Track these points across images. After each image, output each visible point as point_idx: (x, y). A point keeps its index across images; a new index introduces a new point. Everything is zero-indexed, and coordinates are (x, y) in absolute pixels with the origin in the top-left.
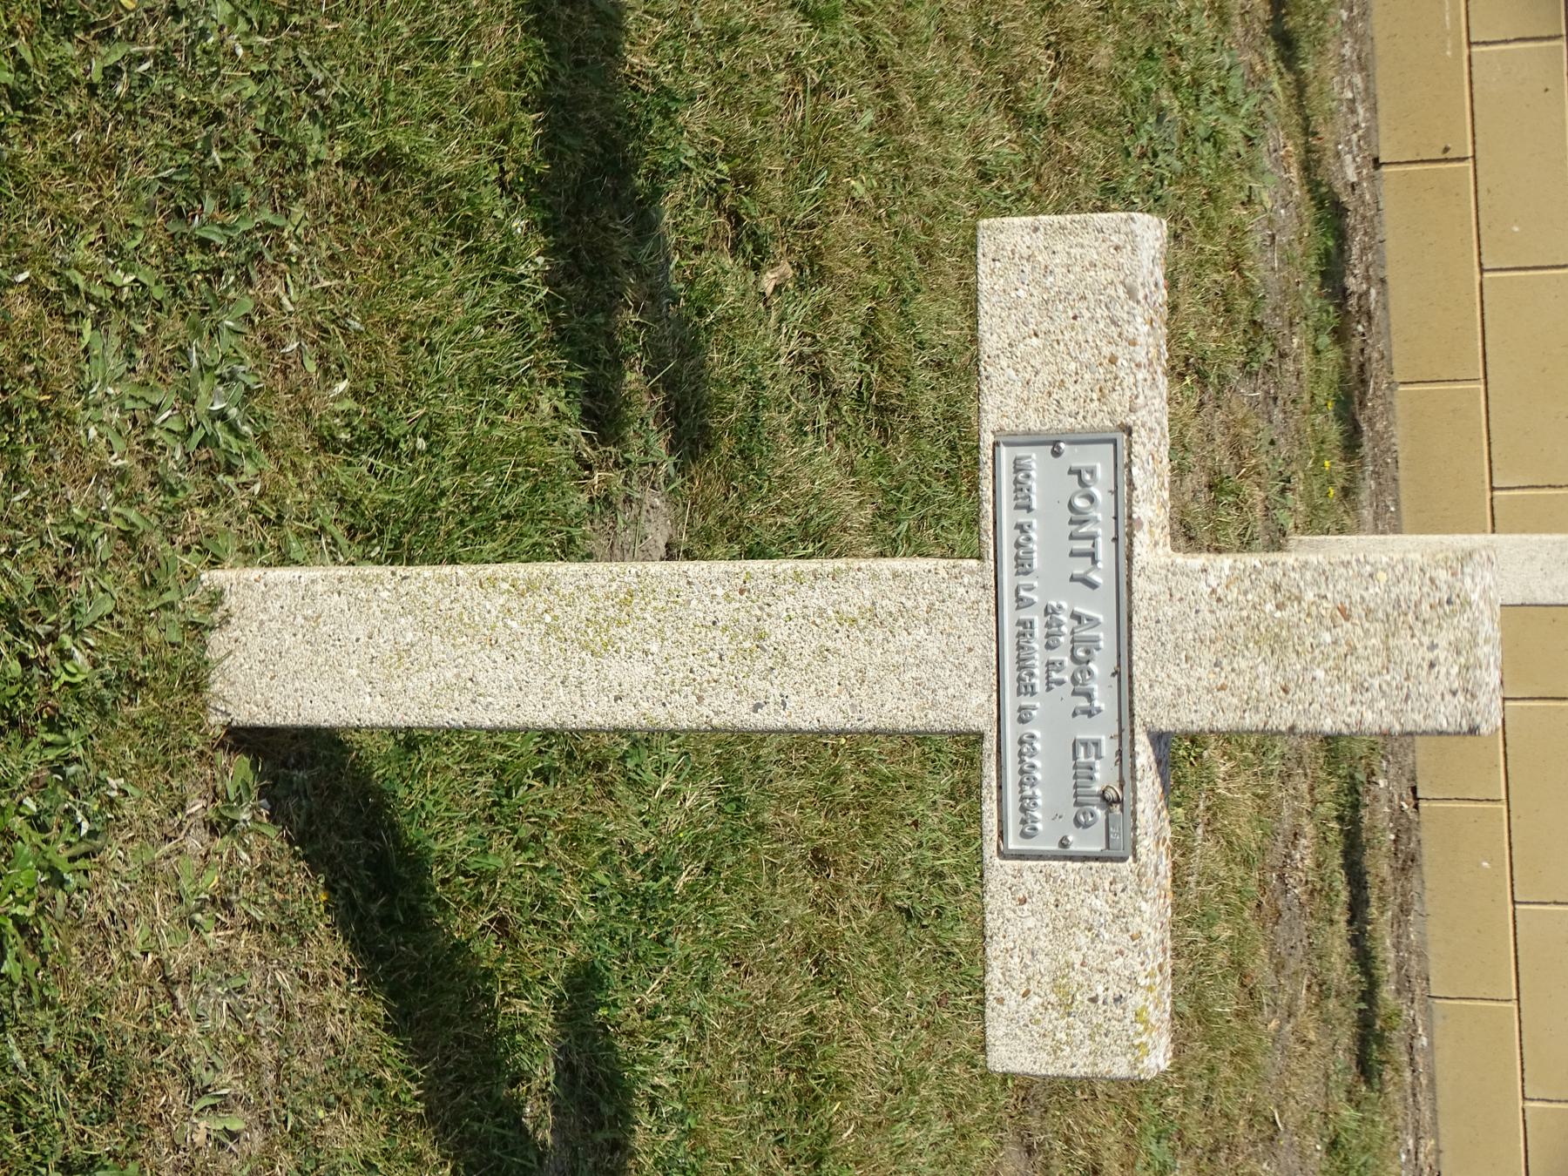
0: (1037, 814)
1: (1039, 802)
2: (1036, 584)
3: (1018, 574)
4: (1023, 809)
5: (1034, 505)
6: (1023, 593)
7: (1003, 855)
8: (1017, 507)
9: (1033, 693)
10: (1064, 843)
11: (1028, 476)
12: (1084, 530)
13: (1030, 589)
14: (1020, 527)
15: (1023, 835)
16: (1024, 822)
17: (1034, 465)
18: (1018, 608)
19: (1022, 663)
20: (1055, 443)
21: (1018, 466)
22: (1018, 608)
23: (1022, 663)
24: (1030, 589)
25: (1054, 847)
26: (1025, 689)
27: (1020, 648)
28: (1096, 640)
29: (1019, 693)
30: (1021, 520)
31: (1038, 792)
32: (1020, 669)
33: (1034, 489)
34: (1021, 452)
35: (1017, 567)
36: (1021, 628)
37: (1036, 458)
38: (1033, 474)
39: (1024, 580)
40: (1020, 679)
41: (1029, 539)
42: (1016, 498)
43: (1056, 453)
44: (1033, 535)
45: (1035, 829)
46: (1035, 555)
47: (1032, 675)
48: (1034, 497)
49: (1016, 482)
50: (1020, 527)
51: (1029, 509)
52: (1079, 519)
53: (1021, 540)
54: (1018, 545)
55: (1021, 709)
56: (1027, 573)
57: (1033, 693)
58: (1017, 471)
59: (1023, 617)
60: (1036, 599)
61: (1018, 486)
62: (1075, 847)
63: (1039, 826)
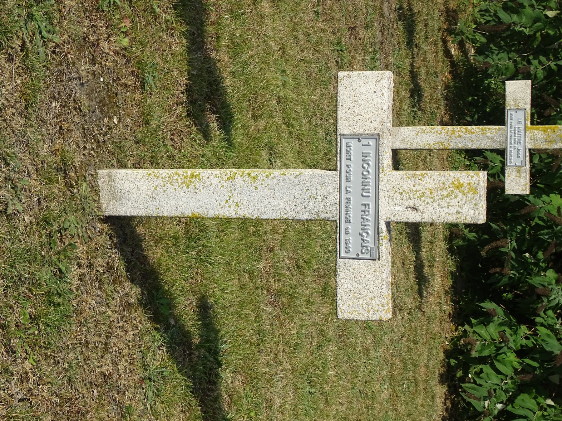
0: (350, 245)
1: (351, 241)
2: (352, 186)
3: (346, 182)
4: (346, 244)
5: (352, 159)
6: (348, 189)
7: (340, 258)
8: (347, 159)
9: (350, 223)
10: (358, 255)
11: (350, 149)
12: (366, 159)
13: (350, 187)
14: (347, 166)
15: (346, 252)
16: (346, 248)
17: (352, 145)
18: (346, 193)
19: (347, 213)
20: (359, 139)
21: (347, 146)
22: (346, 193)
23: (347, 213)
24: (350, 187)
25: (355, 256)
26: (348, 221)
27: (347, 207)
28: (369, 189)
29: (346, 222)
30: (348, 164)
31: (351, 238)
32: (346, 214)
33: (352, 153)
34: (348, 141)
35: (346, 179)
36: (347, 200)
37: (353, 143)
38: (352, 148)
39: (348, 184)
40: (346, 218)
41: (350, 170)
42: (347, 156)
43: (359, 141)
44: (351, 169)
45: (349, 250)
46: (352, 176)
47: (350, 216)
48: (352, 156)
49: (347, 150)
50: (347, 166)
51: (350, 160)
52: (365, 177)
53: (348, 171)
54: (347, 172)
55: (346, 240)
56: (349, 182)
57: (350, 223)
58: (347, 147)
59: (347, 197)
60: (351, 191)
61: (348, 153)
62: (361, 256)
63: (350, 249)
